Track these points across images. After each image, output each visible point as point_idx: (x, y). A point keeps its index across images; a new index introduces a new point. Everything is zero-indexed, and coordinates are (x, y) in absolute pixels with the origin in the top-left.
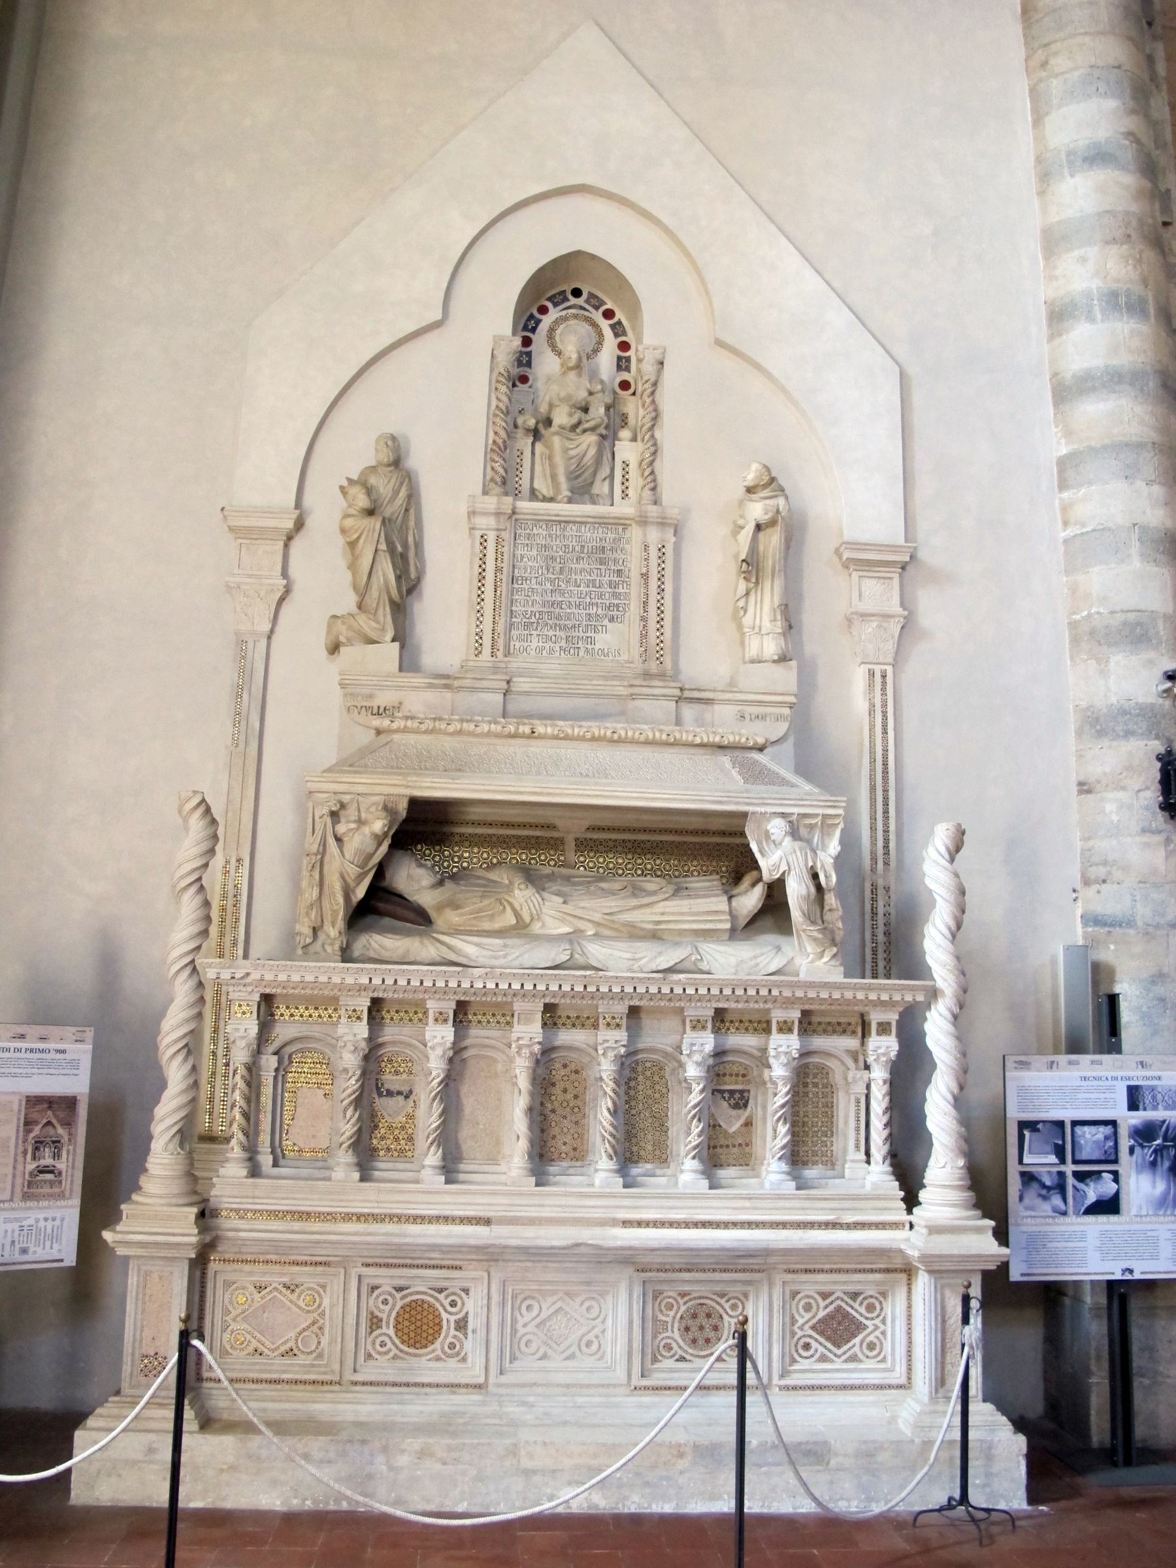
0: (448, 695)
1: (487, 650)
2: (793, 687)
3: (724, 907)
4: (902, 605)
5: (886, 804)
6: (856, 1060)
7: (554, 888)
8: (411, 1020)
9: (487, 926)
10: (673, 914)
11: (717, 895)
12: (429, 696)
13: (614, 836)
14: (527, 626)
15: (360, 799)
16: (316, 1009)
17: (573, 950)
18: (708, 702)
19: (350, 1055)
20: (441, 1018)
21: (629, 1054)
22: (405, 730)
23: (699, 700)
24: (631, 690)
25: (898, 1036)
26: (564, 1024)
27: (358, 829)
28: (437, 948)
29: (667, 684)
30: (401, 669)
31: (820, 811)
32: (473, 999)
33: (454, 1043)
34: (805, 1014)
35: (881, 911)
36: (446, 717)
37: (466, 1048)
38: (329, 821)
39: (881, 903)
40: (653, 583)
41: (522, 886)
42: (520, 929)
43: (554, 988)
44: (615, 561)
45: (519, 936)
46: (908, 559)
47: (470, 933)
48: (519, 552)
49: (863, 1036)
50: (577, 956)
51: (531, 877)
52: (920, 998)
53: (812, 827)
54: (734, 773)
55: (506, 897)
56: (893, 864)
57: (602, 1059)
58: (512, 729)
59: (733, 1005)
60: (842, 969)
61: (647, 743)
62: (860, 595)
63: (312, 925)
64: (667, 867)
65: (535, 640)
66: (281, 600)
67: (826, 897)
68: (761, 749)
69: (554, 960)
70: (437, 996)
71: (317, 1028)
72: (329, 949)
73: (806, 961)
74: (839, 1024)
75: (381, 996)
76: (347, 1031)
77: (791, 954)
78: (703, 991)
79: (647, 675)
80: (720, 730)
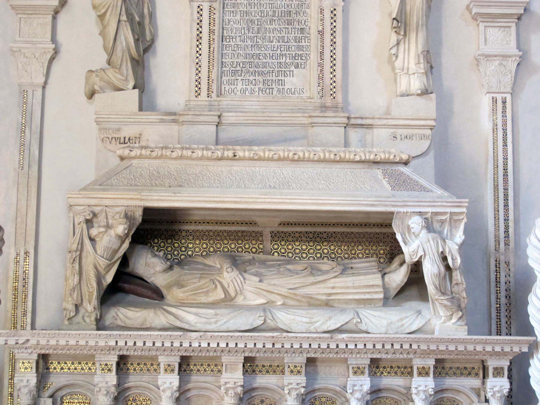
0: (175, 127)
1: (204, 92)
2: (434, 115)
3: (379, 282)
4: (519, 48)
5: (506, 199)
6: (479, 395)
7: (253, 270)
8: (148, 370)
9: (203, 299)
10: (341, 288)
11: (374, 273)
12: (164, 129)
13: (298, 229)
14: (234, 73)
15: (107, 209)
16: (80, 363)
17: (266, 316)
18: (369, 127)
19: (104, 397)
20: (169, 369)
21: (307, 394)
22: (140, 157)
23: (362, 126)
24: (310, 120)
25: (508, 378)
26: (260, 371)
27: (106, 231)
28: (166, 317)
29: (338, 114)
30: (141, 109)
31: (448, 210)
32: (192, 354)
33: (180, 387)
34: (438, 361)
35: (503, 280)
36: (171, 146)
37: (189, 390)
38: (85, 226)
39: (503, 274)
40: (328, 38)
41: (229, 270)
42: (228, 301)
43: (250, 345)
44: (299, 22)
45: (226, 307)
46: (522, 11)
47: (191, 305)
48: (226, 18)
49: (484, 377)
50: (269, 321)
51: (236, 262)
52: (525, 349)
53: (442, 222)
54: (385, 182)
55: (218, 278)
56: (512, 244)
57: (288, 397)
58: (219, 154)
59: (384, 356)
60: (466, 327)
61: (320, 161)
62: (486, 40)
63: (75, 302)
64: (339, 251)
65: (240, 84)
66: (52, 59)
67: (454, 274)
68: (406, 163)
69: (252, 325)
70: (166, 353)
71: (81, 378)
72: (87, 320)
73: (439, 322)
74: (465, 368)
75: (125, 353)
76: (101, 379)
77: (429, 317)
78: (360, 346)
79: (324, 108)
80: (375, 150)
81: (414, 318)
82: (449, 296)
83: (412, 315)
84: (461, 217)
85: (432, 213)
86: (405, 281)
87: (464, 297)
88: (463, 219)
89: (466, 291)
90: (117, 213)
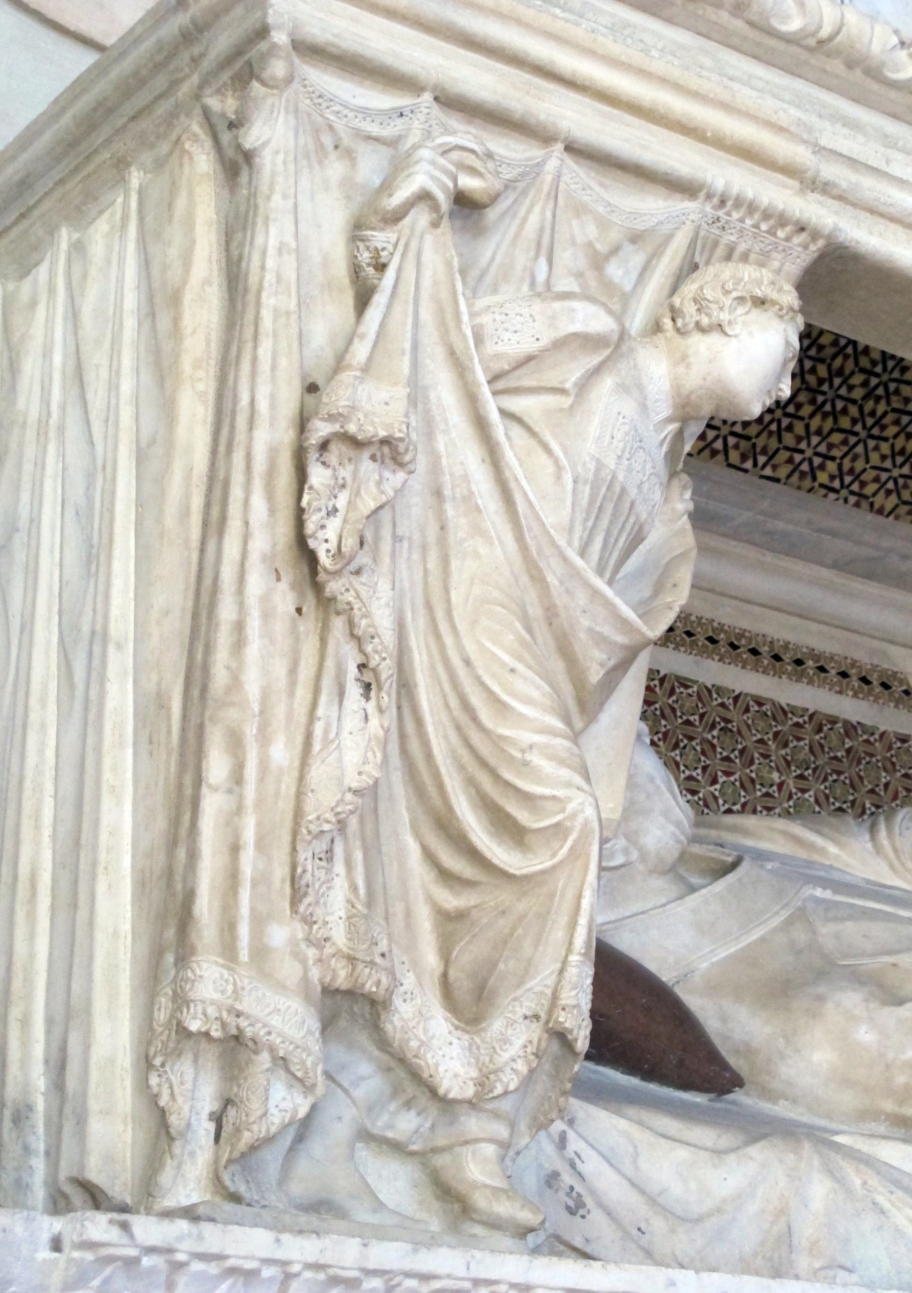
90: (635, 238)
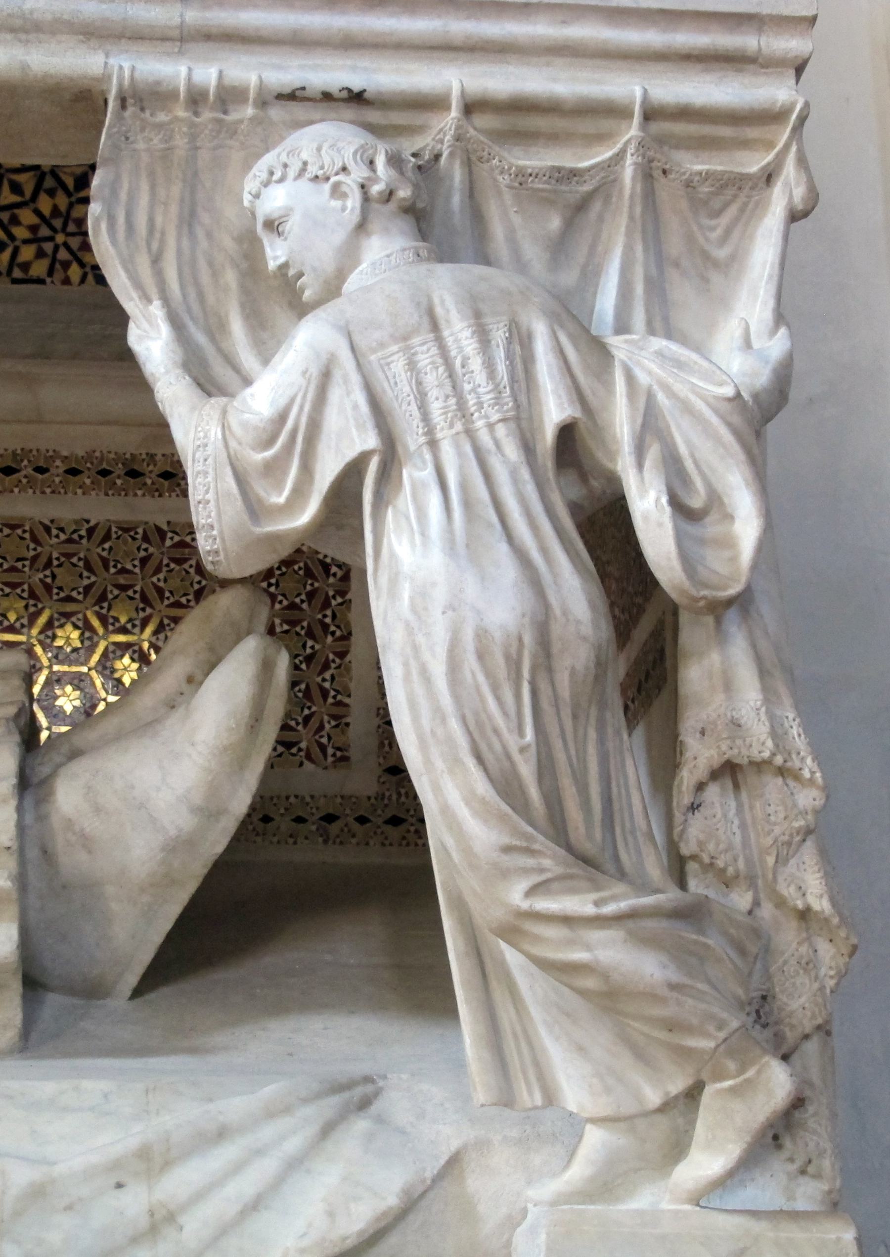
31: (629, 87)
67: (696, 675)
77: (447, 1135)
81: (293, 1145)
82: (643, 887)
83: (271, 1113)
84: (754, 163)
85: (472, 107)
86: (240, 802)
87: (805, 915)
88: (769, 177)
89: (823, 853)
